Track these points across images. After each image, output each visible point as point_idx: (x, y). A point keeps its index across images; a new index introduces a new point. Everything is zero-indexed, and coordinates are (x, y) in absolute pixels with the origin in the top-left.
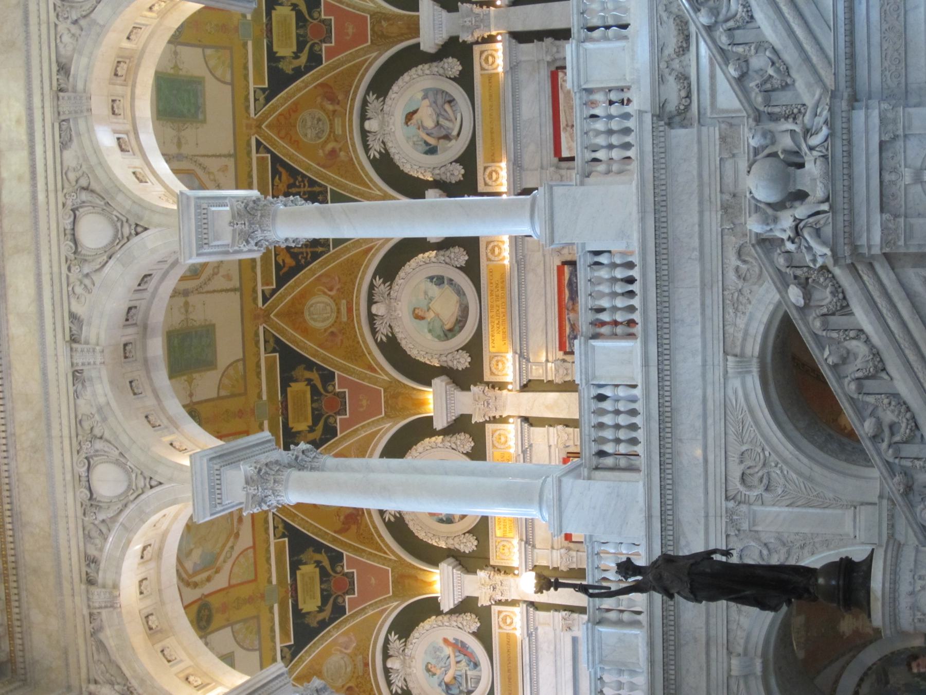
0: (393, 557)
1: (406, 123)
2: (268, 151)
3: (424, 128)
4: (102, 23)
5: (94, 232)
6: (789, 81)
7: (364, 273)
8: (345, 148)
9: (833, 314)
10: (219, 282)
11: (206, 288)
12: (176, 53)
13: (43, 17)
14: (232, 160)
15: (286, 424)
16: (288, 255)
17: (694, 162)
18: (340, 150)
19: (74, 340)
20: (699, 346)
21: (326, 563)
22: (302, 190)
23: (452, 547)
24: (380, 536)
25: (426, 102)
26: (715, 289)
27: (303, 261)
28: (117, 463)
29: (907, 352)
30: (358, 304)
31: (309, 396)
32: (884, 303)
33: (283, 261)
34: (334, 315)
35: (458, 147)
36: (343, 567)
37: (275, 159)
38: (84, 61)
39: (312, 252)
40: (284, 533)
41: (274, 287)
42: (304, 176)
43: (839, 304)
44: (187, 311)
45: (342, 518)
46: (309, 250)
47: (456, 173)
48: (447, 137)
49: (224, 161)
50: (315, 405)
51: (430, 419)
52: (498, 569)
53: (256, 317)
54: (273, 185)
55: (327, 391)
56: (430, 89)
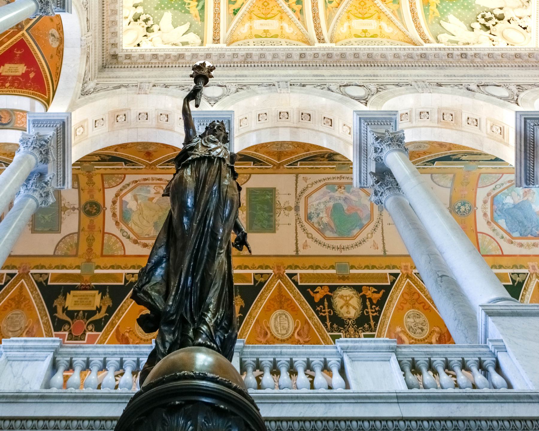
11: (299, 229)
16: (322, 297)
21: (97, 317)
22: (370, 310)
27: (319, 309)
33: (318, 292)
36: (91, 331)
39: (325, 316)
41: (299, 284)
44: (285, 209)
46: (327, 314)
49: (381, 246)
53: (279, 268)
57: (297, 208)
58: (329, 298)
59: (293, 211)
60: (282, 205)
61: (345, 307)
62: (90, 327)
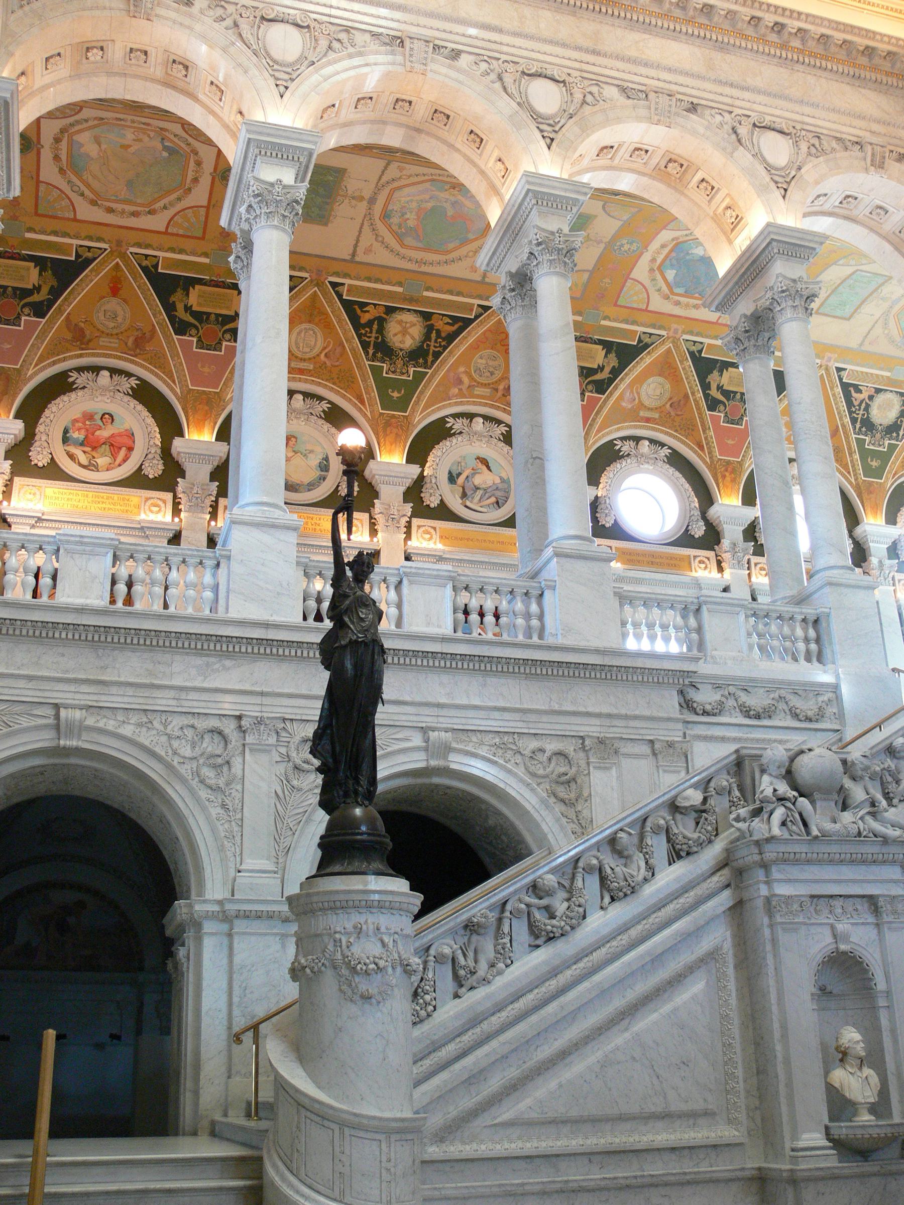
0: (30, 373)
1: (478, 458)
2: (477, 317)
3: (473, 475)
4: (735, 154)
5: (546, 97)
6: (895, 801)
7: (337, 393)
8: (461, 394)
9: (668, 841)
10: (367, 239)
12: (600, 242)
13: (737, 103)
14: (479, 279)
15: (200, 281)
17: (647, 713)
18: (460, 390)
19: (436, 48)
20: (458, 701)
21: (36, 298)
23: (37, 438)
24: (54, 363)
25: (498, 481)
26: (519, 724)
28: (302, 58)
29: (639, 927)
30: (306, 381)
31: (224, 312)
32: (690, 900)
34: (300, 355)
35: (455, 504)
36: (29, 315)
37: (467, 322)
38: (701, 130)
40: (80, 256)
42: (445, 348)
43: (684, 847)
44: (353, 198)
45: (82, 325)
46: (373, 339)
47: (432, 499)
48: (464, 495)
50: (213, 317)
51: (182, 435)
52: (9, 485)
54: (444, 315)
55: (225, 332)
56: (510, 486)
57: (372, 201)
58: (381, 321)
59: (365, 203)
60: (350, 192)
61: (399, 336)
62: (26, 311)
